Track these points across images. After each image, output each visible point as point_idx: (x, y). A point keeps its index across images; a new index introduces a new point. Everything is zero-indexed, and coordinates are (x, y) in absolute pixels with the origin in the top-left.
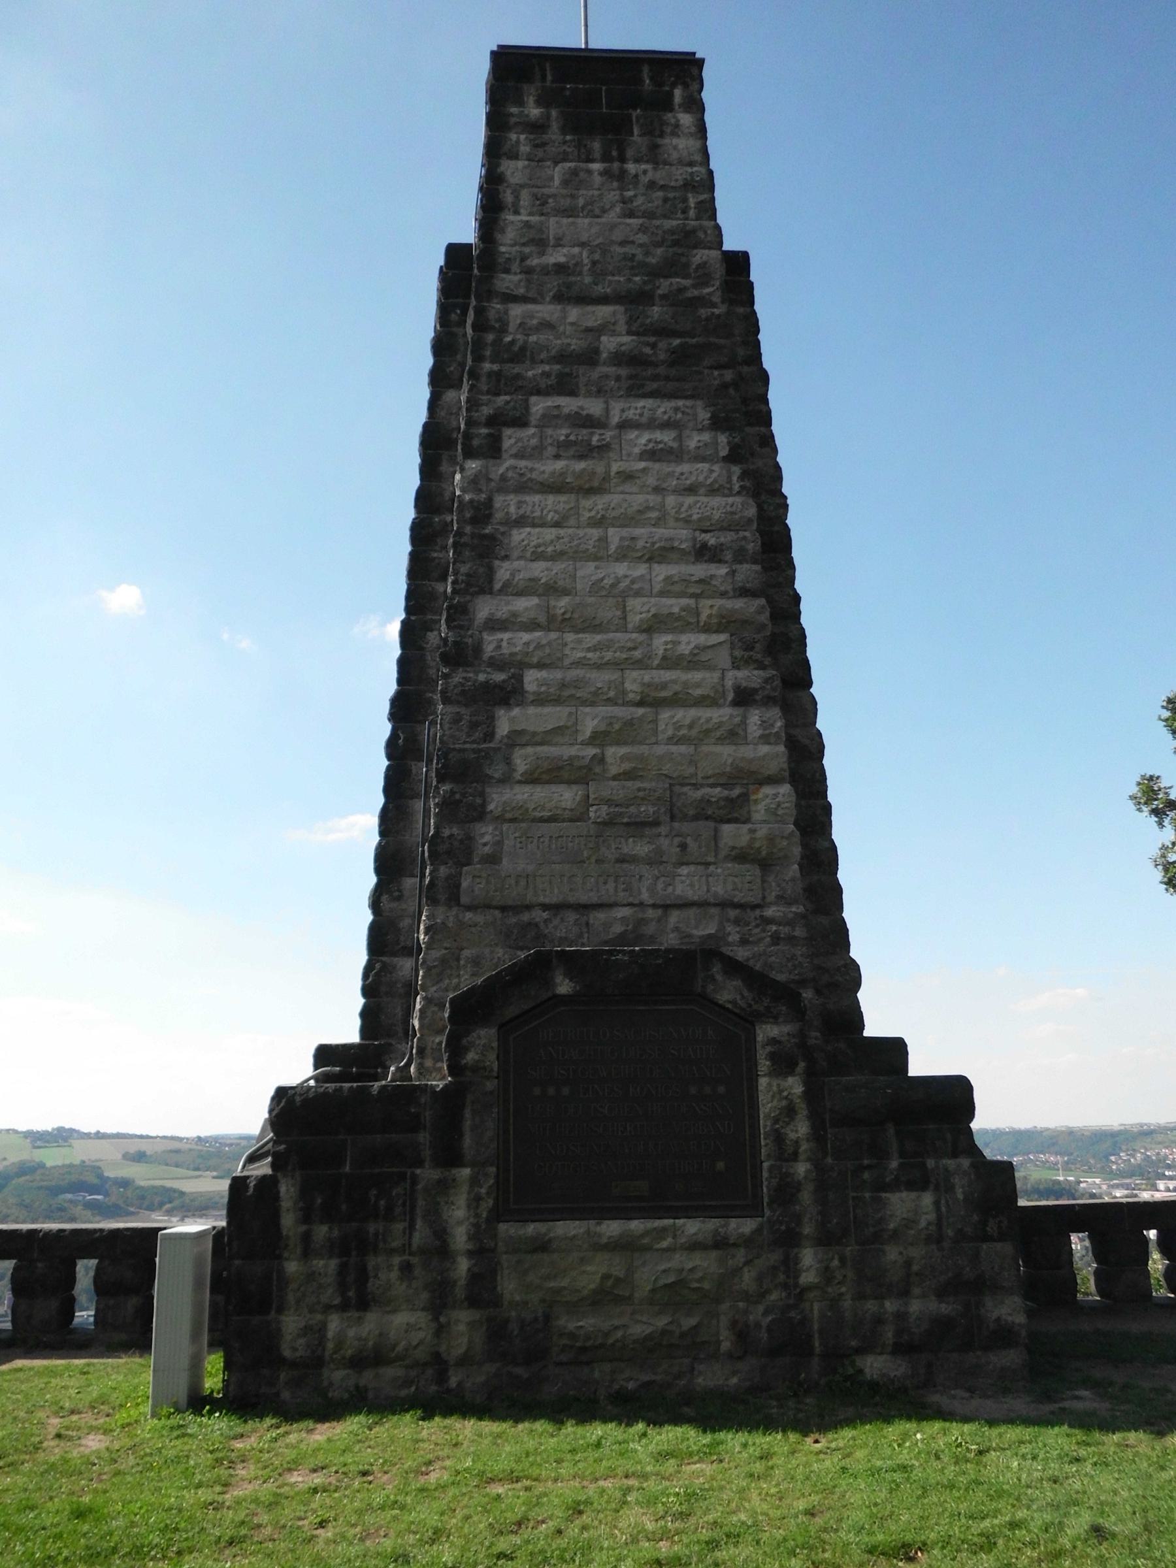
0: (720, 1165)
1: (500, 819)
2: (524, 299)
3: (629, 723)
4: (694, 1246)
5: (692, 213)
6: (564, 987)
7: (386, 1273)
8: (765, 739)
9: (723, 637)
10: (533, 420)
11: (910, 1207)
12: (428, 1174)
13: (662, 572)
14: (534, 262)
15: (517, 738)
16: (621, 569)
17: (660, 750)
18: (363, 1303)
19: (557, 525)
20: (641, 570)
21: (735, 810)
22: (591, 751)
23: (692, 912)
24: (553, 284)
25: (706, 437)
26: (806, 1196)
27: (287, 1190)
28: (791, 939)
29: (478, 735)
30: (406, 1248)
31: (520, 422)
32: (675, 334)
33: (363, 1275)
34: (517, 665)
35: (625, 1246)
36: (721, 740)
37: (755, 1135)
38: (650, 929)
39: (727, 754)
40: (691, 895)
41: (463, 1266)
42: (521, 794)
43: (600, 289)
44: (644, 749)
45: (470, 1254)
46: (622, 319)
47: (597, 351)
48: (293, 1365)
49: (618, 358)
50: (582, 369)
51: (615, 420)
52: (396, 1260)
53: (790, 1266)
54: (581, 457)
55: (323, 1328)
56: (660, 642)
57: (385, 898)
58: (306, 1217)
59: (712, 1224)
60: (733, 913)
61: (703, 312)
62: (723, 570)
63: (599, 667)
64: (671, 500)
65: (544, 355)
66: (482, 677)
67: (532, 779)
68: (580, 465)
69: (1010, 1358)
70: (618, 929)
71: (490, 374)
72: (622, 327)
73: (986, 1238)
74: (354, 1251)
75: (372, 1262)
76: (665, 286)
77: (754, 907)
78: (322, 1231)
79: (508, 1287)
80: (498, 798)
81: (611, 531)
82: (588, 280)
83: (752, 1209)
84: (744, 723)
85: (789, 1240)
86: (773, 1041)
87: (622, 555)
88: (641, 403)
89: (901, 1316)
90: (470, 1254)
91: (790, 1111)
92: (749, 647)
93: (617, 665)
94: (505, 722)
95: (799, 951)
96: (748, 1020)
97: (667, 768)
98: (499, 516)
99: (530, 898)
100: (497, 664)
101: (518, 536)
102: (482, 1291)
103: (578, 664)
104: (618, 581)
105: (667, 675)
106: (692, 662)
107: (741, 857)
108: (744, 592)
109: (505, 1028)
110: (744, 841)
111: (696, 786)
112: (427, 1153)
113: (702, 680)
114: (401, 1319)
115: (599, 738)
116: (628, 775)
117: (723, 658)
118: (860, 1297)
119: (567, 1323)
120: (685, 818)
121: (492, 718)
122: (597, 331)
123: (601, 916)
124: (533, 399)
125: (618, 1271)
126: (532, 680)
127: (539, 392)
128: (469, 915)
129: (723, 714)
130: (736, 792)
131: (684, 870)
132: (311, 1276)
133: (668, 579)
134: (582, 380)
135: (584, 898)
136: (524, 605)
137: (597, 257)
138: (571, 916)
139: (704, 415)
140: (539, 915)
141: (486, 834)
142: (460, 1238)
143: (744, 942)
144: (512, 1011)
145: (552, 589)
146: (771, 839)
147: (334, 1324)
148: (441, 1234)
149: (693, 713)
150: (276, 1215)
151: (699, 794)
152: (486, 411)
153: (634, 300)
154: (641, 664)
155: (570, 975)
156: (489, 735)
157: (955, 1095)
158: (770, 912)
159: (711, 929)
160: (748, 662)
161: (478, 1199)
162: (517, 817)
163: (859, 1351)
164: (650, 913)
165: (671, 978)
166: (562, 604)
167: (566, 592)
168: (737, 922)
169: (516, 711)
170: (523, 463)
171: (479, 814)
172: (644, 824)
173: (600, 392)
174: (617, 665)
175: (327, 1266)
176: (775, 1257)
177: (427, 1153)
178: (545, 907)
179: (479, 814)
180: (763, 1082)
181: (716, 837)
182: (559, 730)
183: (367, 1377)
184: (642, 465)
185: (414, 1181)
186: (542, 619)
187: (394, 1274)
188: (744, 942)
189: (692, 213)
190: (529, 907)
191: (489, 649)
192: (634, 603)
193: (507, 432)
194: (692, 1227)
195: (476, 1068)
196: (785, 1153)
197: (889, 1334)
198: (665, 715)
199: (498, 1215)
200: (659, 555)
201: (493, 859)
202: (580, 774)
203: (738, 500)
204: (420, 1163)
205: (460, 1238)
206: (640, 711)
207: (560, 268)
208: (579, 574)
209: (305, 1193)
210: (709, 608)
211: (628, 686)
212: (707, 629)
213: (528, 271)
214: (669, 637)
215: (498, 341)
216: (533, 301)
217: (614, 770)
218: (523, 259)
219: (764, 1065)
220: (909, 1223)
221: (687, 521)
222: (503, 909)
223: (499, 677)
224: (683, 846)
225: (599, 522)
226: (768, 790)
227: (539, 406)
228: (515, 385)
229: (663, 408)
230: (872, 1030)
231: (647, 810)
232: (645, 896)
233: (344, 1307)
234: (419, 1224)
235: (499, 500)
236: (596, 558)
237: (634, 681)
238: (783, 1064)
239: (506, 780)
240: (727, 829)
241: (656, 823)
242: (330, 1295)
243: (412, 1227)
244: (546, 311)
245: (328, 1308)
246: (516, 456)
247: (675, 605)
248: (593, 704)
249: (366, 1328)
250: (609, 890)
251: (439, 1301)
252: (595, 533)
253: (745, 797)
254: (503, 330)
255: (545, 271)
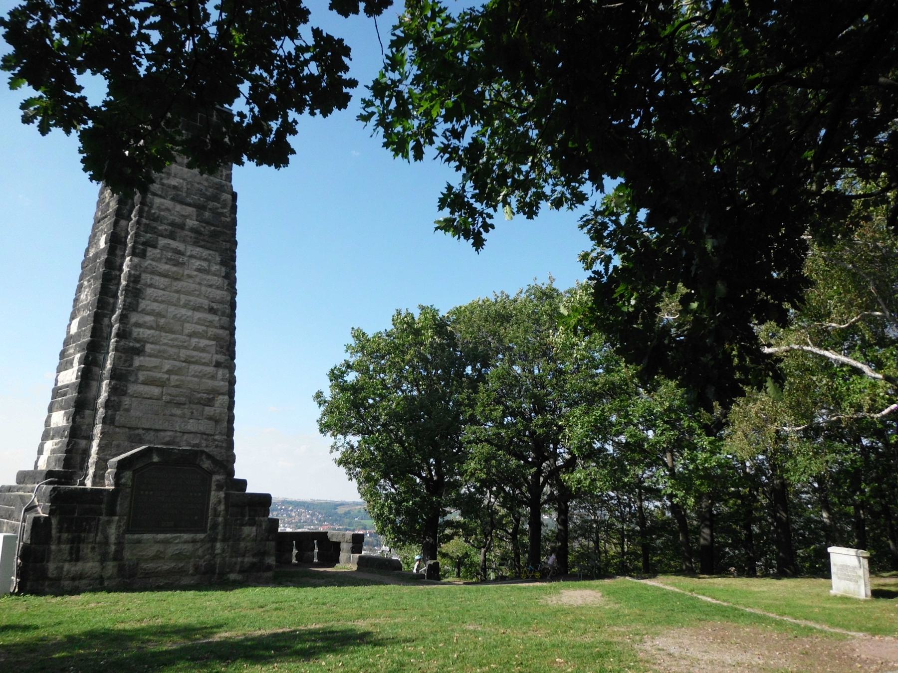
0: (196, 518)
1: (132, 396)
2: (161, 196)
3: (180, 369)
4: (186, 542)
5: (224, 178)
6: (156, 459)
7: (86, 550)
8: (223, 380)
9: (214, 343)
10: (159, 246)
11: (249, 531)
12: (104, 518)
13: (198, 315)
14: (165, 181)
15: (141, 368)
16: (183, 311)
17: (189, 378)
18: (77, 559)
19: (163, 289)
20: (190, 313)
21: (209, 402)
22: (166, 376)
23: (191, 435)
24: (172, 193)
25: (218, 267)
26: (220, 527)
27: (54, 521)
28: (221, 447)
29: (127, 364)
30: (94, 542)
31: (155, 246)
32: (213, 225)
33: (78, 551)
34: (144, 342)
35: (166, 542)
36: (209, 378)
37: (208, 509)
38: (178, 440)
39: (210, 383)
40: (193, 430)
41: (113, 548)
42: (141, 388)
43: (189, 200)
44: (184, 377)
45: (115, 544)
46: (195, 214)
47: (184, 225)
48: (51, 579)
49: (192, 230)
50: (178, 230)
51: (188, 253)
52: (90, 546)
53: (213, 548)
54: (175, 265)
55: (62, 568)
56: (194, 341)
57: (78, 417)
58: (60, 531)
59: (192, 535)
60: (205, 437)
61: (223, 219)
62: (217, 318)
63: (171, 346)
64: (203, 288)
65: (165, 222)
66: (131, 344)
67: (145, 383)
68: (175, 269)
69: (270, 574)
70: (168, 439)
71: (145, 224)
72: (194, 218)
73: (268, 540)
74: (76, 544)
75: (81, 546)
76: (211, 204)
77: (211, 435)
78: (65, 536)
79: (127, 554)
80: (132, 388)
81: (182, 296)
82: (184, 195)
83: (204, 531)
84: (217, 374)
85: (214, 540)
86: (218, 481)
87: (185, 306)
88: (198, 249)
89: (242, 562)
90: (115, 544)
91: (219, 502)
92: (222, 348)
93: (178, 347)
94: (137, 361)
95: (223, 451)
96: (210, 473)
97: (190, 386)
98: (142, 282)
99: (139, 425)
100: (137, 340)
101: (149, 291)
102: (118, 556)
103: (165, 344)
104: (183, 315)
105: (195, 353)
106: (203, 350)
107: (210, 418)
108: (222, 328)
109: (134, 472)
110: (212, 413)
111: (199, 393)
112: (104, 511)
113: (206, 357)
114: (90, 564)
115: (169, 372)
116: (177, 386)
117: (213, 350)
118: (231, 557)
119: (144, 565)
120: (194, 403)
121: (132, 359)
122: (186, 217)
123: (162, 433)
124: (160, 238)
125: (162, 549)
126: (149, 348)
127: (162, 236)
128: (117, 430)
129: (210, 369)
130: (211, 396)
131: (191, 421)
132: (60, 550)
133: (199, 319)
134: (178, 235)
135: (157, 427)
136: (148, 319)
137: (189, 186)
138: (152, 433)
139: (218, 259)
140: (141, 432)
141: (126, 401)
142: (112, 539)
143: (207, 446)
144: (137, 467)
145: (159, 315)
146: (220, 414)
147: (66, 566)
148: (106, 538)
149: (201, 368)
150: (51, 530)
151: (199, 396)
152: (142, 239)
153: (200, 208)
154: (186, 348)
155: (158, 455)
156: (131, 365)
157: (264, 500)
158: (216, 437)
159: (197, 441)
160: (221, 352)
161: (120, 526)
162: (139, 396)
163: (229, 573)
164: (178, 434)
165: (191, 458)
166: (162, 321)
167: (164, 317)
168: (205, 440)
169: (142, 358)
170: (154, 263)
171: (124, 393)
172: (180, 404)
173: (184, 241)
174: (178, 347)
175: (66, 547)
176: (208, 545)
177: (104, 511)
178: (144, 429)
179: (124, 393)
180: (213, 493)
181: (203, 411)
182: (155, 367)
183: (76, 583)
184: (196, 273)
185: (99, 520)
186: (154, 326)
187: (89, 550)
188: (207, 446)
189: (224, 178)
190: (138, 429)
191: (135, 335)
192: (187, 325)
193: (149, 249)
194: (186, 536)
195: (125, 484)
196: (216, 514)
197: (238, 567)
198: (192, 367)
199: (128, 531)
200: (196, 309)
201: (128, 410)
202: (161, 384)
203: (225, 293)
204: (101, 514)
205: (112, 539)
206: (184, 364)
207: (175, 187)
208: (169, 310)
209: (60, 523)
210: (212, 331)
211: (181, 355)
212: (209, 339)
213: (163, 184)
214: (197, 340)
215: (149, 211)
216: (164, 198)
217: (173, 384)
218: (161, 179)
219: (214, 487)
220: (249, 535)
221: (208, 297)
222: (129, 428)
223: (138, 345)
224: (192, 413)
225: (178, 292)
226: (221, 397)
227: (162, 242)
228: (153, 230)
229: (205, 253)
230: (237, 476)
231: (183, 399)
232: (178, 428)
233: (70, 561)
234: (99, 534)
235: (144, 276)
236: (175, 305)
237: (183, 353)
238: (219, 487)
239: (136, 382)
240: (207, 408)
241: (185, 404)
242: (66, 556)
243: (96, 535)
244: (168, 203)
245: (65, 561)
246: (152, 260)
247: (200, 329)
248: (168, 359)
249: (79, 567)
250: (166, 426)
251: (103, 559)
252: (176, 295)
253: (213, 398)
254: (151, 207)
255: (169, 186)
